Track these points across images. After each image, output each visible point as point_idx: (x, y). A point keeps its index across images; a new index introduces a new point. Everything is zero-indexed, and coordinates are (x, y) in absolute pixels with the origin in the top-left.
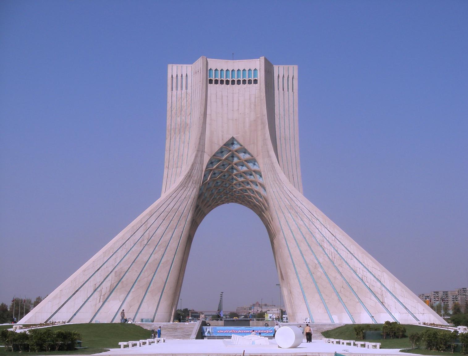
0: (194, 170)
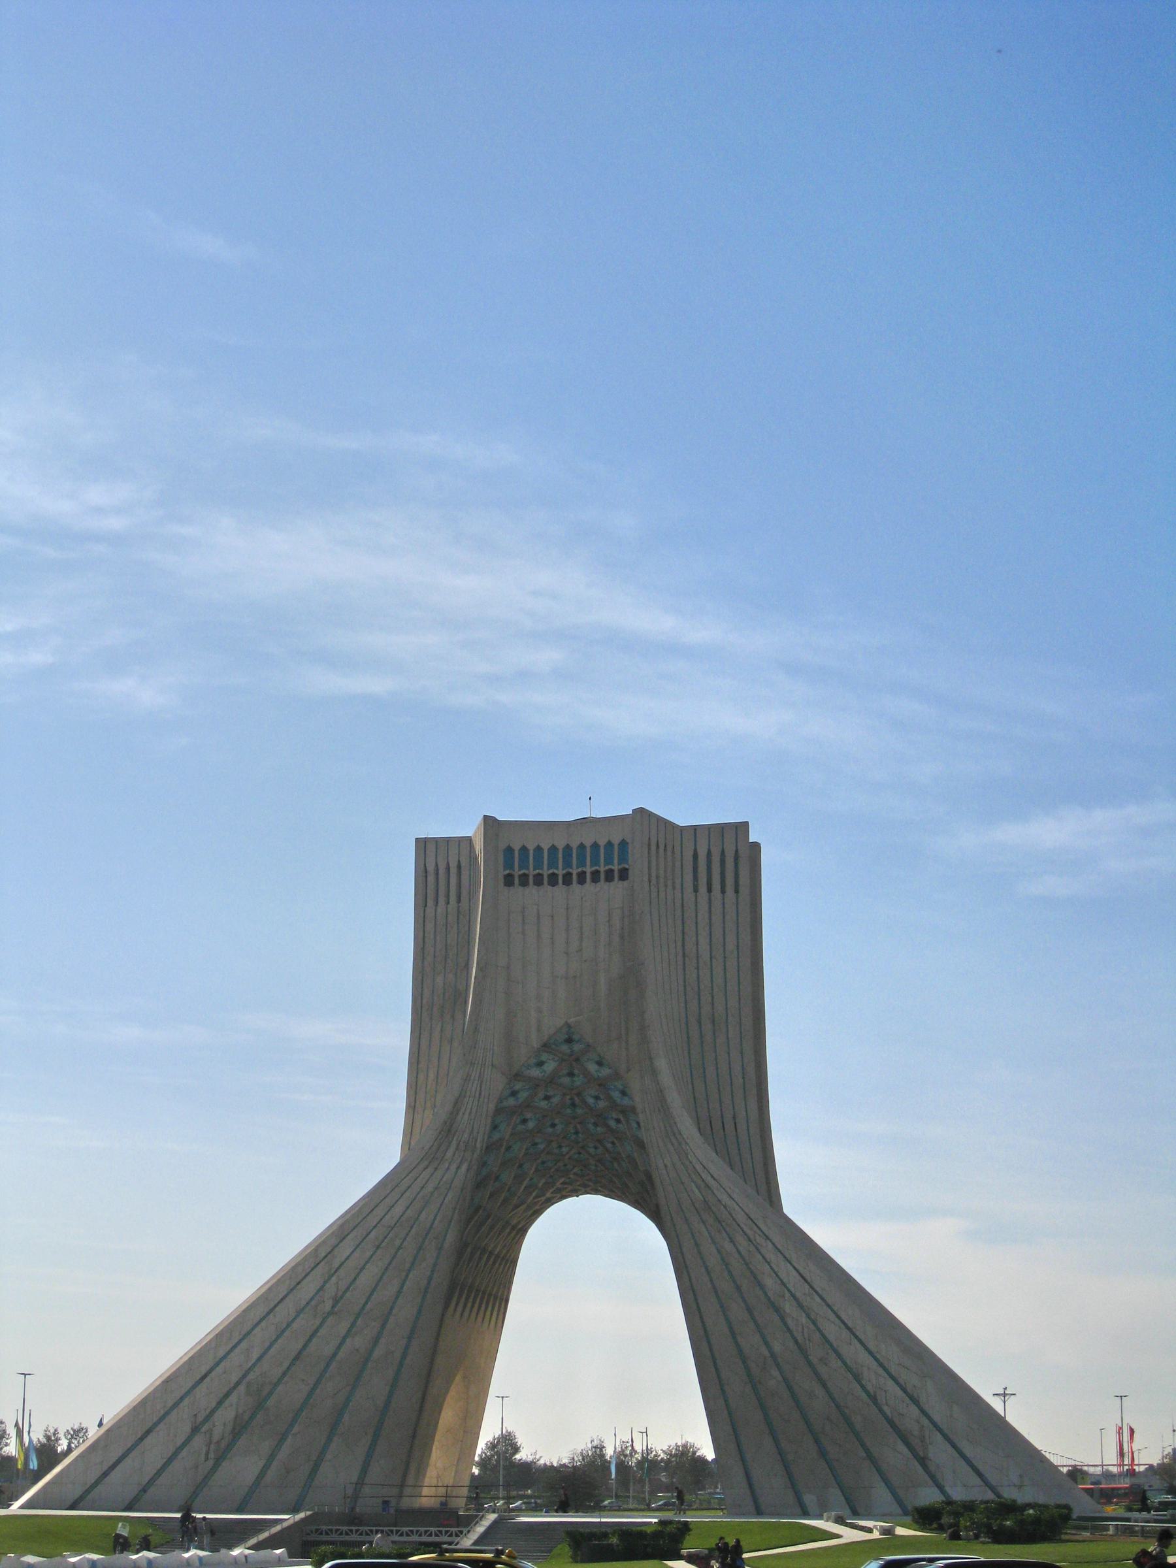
0: (459, 1118)
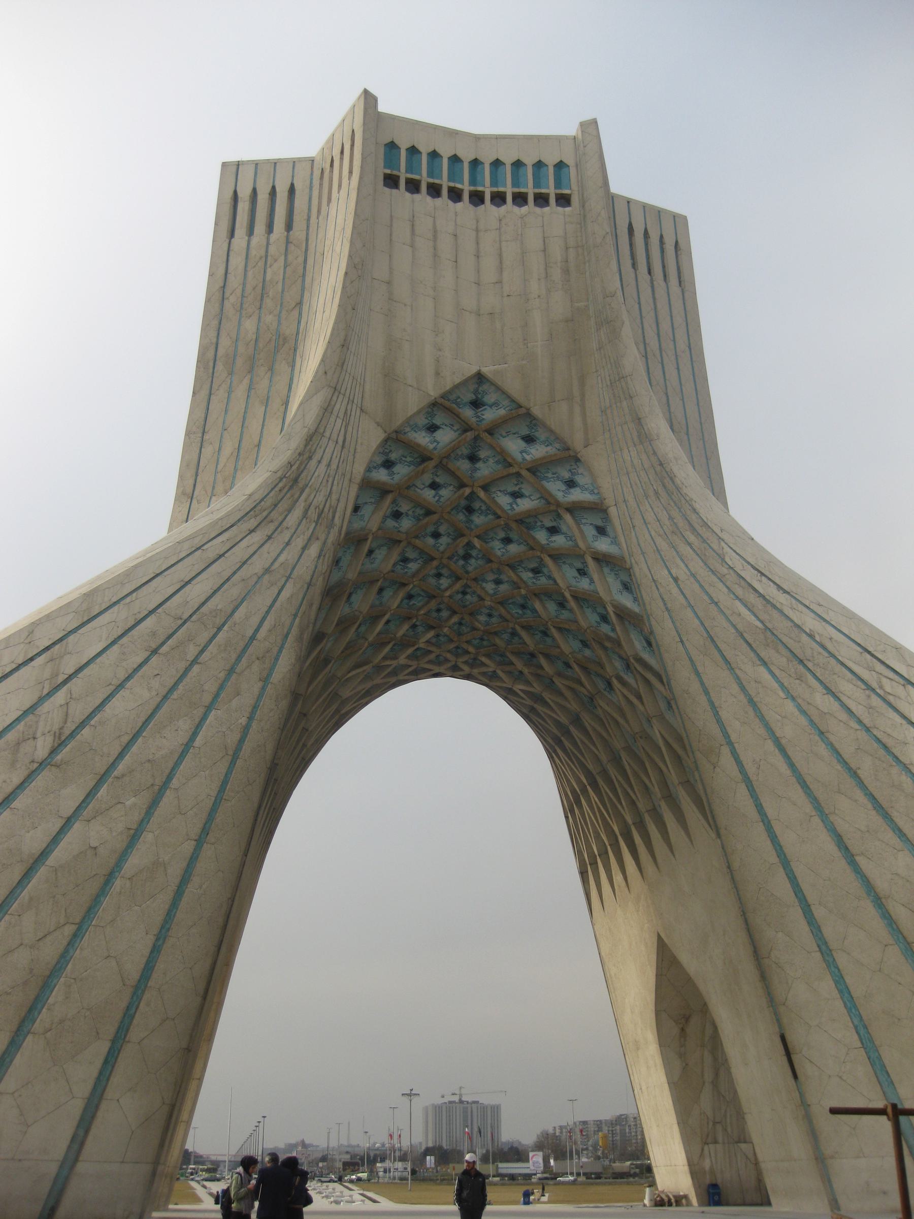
0: (313, 463)
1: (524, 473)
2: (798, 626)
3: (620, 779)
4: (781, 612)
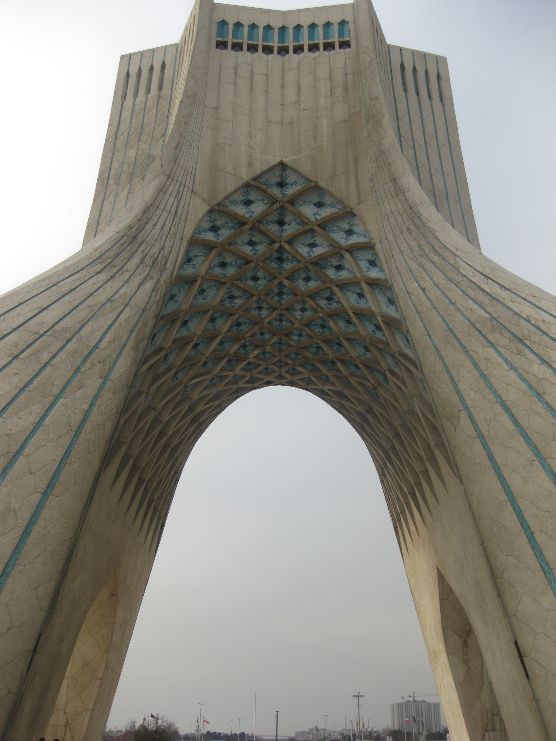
0: (150, 226)
1: (316, 228)
2: (517, 314)
3: (402, 450)
4: (504, 304)
